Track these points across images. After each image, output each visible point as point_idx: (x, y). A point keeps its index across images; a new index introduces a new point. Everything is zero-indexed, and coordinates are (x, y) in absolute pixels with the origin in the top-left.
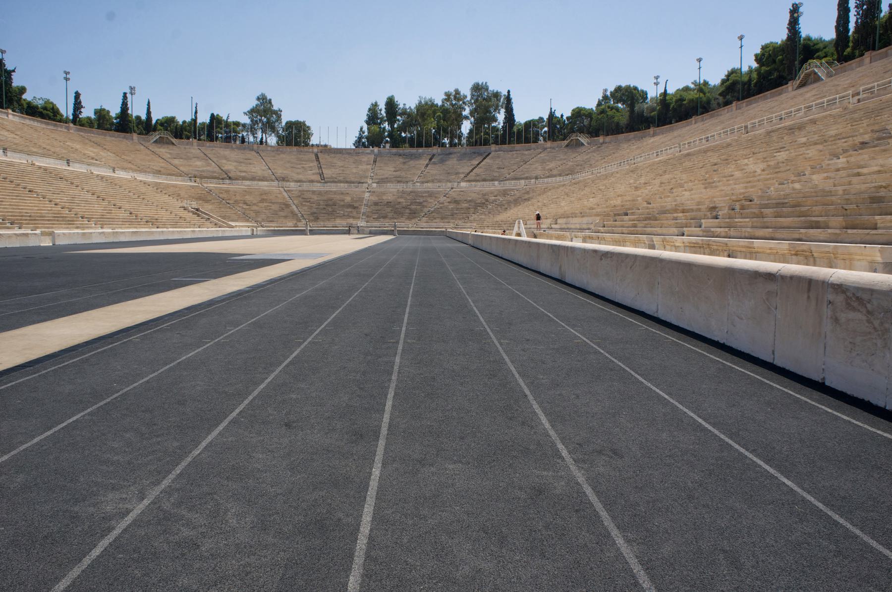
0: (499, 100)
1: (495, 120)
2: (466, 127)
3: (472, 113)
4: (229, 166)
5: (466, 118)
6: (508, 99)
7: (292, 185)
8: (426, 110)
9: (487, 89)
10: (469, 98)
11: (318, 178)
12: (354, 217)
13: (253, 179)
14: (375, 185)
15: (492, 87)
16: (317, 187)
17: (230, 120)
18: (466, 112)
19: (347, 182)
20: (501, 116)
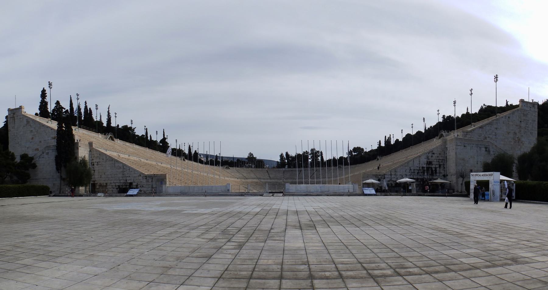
0: (319, 153)
1: (318, 159)
2: (310, 160)
3: (311, 157)
4: (245, 175)
5: (310, 159)
6: (321, 153)
7: (263, 180)
8: (299, 156)
9: (315, 150)
10: (310, 153)
11: (269, 178)
12: (280, 189)
13: (252, 178)
14: (285, 180)
15: (317, 149)
16: (269, 181)
17: (243, 160)
18: (310, 157)
19: (277, 179)
20: (319, 158)
